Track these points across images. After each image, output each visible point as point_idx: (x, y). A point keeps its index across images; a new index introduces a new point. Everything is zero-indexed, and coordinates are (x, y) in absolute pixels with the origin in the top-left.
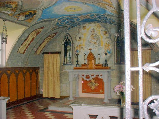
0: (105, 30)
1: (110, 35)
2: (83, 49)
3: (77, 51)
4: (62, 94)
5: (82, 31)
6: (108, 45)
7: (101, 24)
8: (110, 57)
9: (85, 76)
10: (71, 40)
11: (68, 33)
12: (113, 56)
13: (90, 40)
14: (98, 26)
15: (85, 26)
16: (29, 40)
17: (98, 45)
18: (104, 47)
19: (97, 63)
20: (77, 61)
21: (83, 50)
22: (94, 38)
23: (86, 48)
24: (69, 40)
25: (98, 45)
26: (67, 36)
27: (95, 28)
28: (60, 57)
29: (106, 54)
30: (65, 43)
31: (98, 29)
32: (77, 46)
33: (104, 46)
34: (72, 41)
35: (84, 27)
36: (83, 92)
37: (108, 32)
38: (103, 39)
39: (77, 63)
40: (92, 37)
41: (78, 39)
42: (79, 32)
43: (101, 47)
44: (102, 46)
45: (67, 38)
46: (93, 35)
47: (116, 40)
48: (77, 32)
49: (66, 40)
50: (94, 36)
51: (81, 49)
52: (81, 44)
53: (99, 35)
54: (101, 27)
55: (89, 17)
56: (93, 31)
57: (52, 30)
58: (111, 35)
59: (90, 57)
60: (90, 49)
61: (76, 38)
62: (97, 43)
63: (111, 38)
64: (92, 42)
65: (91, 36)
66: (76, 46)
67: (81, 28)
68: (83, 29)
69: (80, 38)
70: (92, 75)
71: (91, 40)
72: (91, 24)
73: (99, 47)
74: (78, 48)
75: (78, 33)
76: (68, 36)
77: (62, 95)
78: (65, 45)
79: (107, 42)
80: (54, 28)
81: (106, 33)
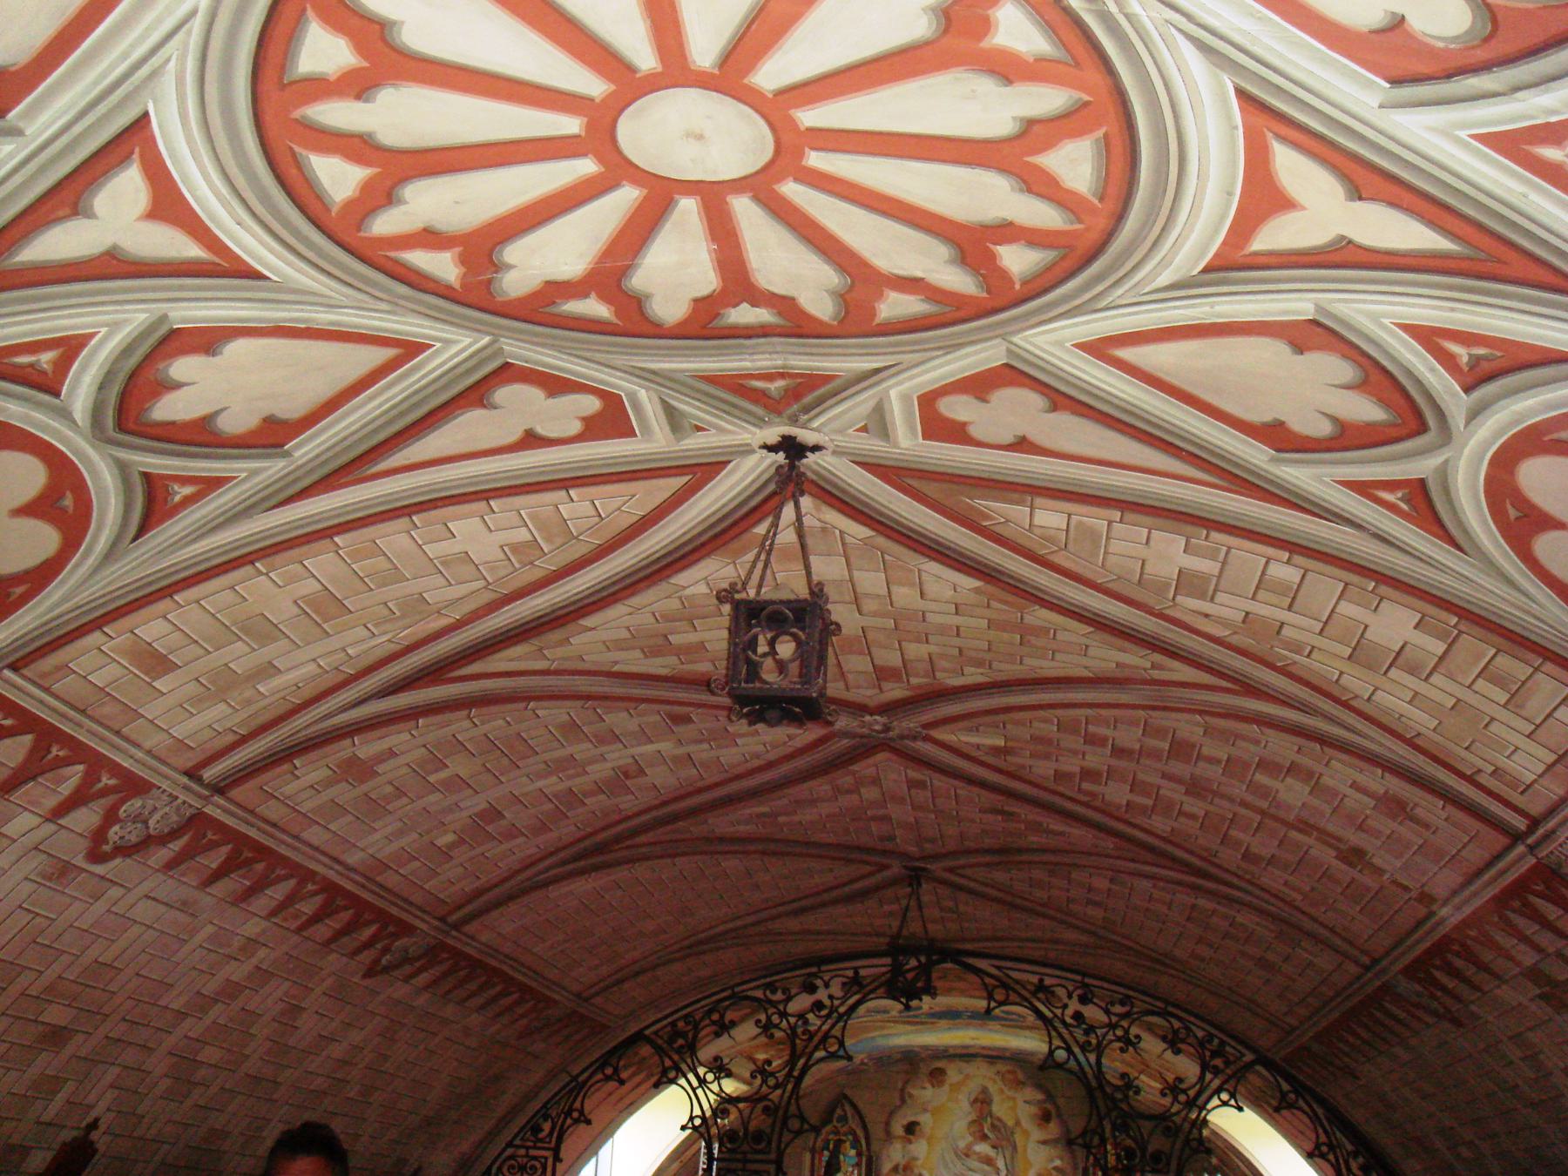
0: (1044, 1101)
5: (926, 1093)
10: (860, 1133)
11: (848, 1092)
13: (962, 1144)
14: (1010, 1076)
22: (984, 1137)
27: (993, 1089)
31: (1006, 1090)
34: (867, 1138)
35: (937, 1076)
37: (1059, 1115)
41: (898, 1129)
42: (911, 1096)
45: (843, 1119)
46: (977, 1123)
48: (897, 1095)
50: (985, 1122)
53: (1010, 1123)
56: (982, 1101)
61: (887, 1124)
62: (1001, 1164)
64: (975, 1157)
68: (928, 1085)
69: (911, 1129)
71: (969, 1147)
75: (903, 1101)
79: (1052, 1160)
81: (1045, 1117)
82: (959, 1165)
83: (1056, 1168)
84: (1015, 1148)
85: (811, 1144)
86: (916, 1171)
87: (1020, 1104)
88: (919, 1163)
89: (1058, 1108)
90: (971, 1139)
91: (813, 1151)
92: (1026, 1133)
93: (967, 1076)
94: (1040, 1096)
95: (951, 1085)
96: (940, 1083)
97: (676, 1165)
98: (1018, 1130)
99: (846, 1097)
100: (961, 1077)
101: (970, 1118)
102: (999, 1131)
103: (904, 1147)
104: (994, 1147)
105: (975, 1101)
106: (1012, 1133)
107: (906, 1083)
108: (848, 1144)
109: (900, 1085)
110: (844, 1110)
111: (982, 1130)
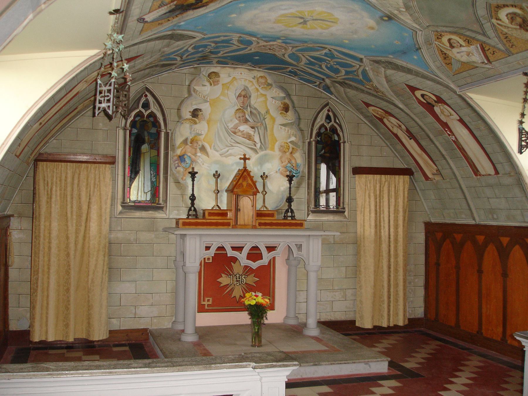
0: (284, 98)
1: (299, 116)
2: (207, 154)
3: (181, 158)
4: (114, 321)
6: (291, 150)
7: (269, 74)
8: (298, 187)
9: (245, 251)
11: (150, 87)
12: (305, 185)
13: (231, 125)
14: (261, 80)
15: (216, 74)
16: (66, 98)
17: (258, 145)
18: (277, 153)
19: (259, 205)
20: (193, 198)
21: (204, 157)
22: (246, 121)
23: (217, 151)
24: (152, 115)
25: (258, 145)
26: (143, 99)
27: (251, 89)
28: (114, 180)
29: (290, 178)
30: (133, 124)
31: (259, 89)
32: (185, 142)
33: (280, 150)
35: (213, 76)
36: (201, 309)
37: (294, 107)
38: (275, 126)
39: (193, 204)
40: (241, 115)
41: (186, 114)
42: (194, 90)
43: (268, 152)
44: (273, 149)
45: (146, 106)
47: (316, 138)
49: (140, 114)
51: (199, 154)
52: (201, 135)
53: (263, 112)
54: (270, 85)
55: (285, 54)
57: (137, 71)
58: (300, 119)
59: (245, 184)
60: (245, 159)
61: (179, 109)
62: (257, 139)
63: (302, 126)
64: (240, 134)
65: (236, 113)
66: (179, 141)
67: (201, 75)
68: (208, 84)
69: (195, 113)
70: (270, 249)
72: (237, 69)
73: (261, 153)
74: (189, 149)
76: (150, 98)
77: (117, 328)
78: (135, 131)
79: (290, 137)
80: (147, 65)
81: (286, 109)
82: (229, 139)
83: (292, 142)
84: (266, 128)
85: (123, 125)
86: (200, 143)
87: (270, 99)
88: (202, 137)
89: (293, 102)
90: (237, 122)
91: (125, 129)
92: (274, 120)
93: (234, 78)
94: (282, 95)
95: (223, 84)
96: (216, 83)
97: (36, 126)
98: (267, 116)
99: (147, 90)
100: (231, 78)
101: (236, 108)
102: (255, 115)
103: (191, 126)
104: (252, 128)
105: (240, 96)
106: (264, 119)
107: (192, 81)
108: (150, 125)
109: (187, 83)
110: (147, 100)
111: (244, 116)
